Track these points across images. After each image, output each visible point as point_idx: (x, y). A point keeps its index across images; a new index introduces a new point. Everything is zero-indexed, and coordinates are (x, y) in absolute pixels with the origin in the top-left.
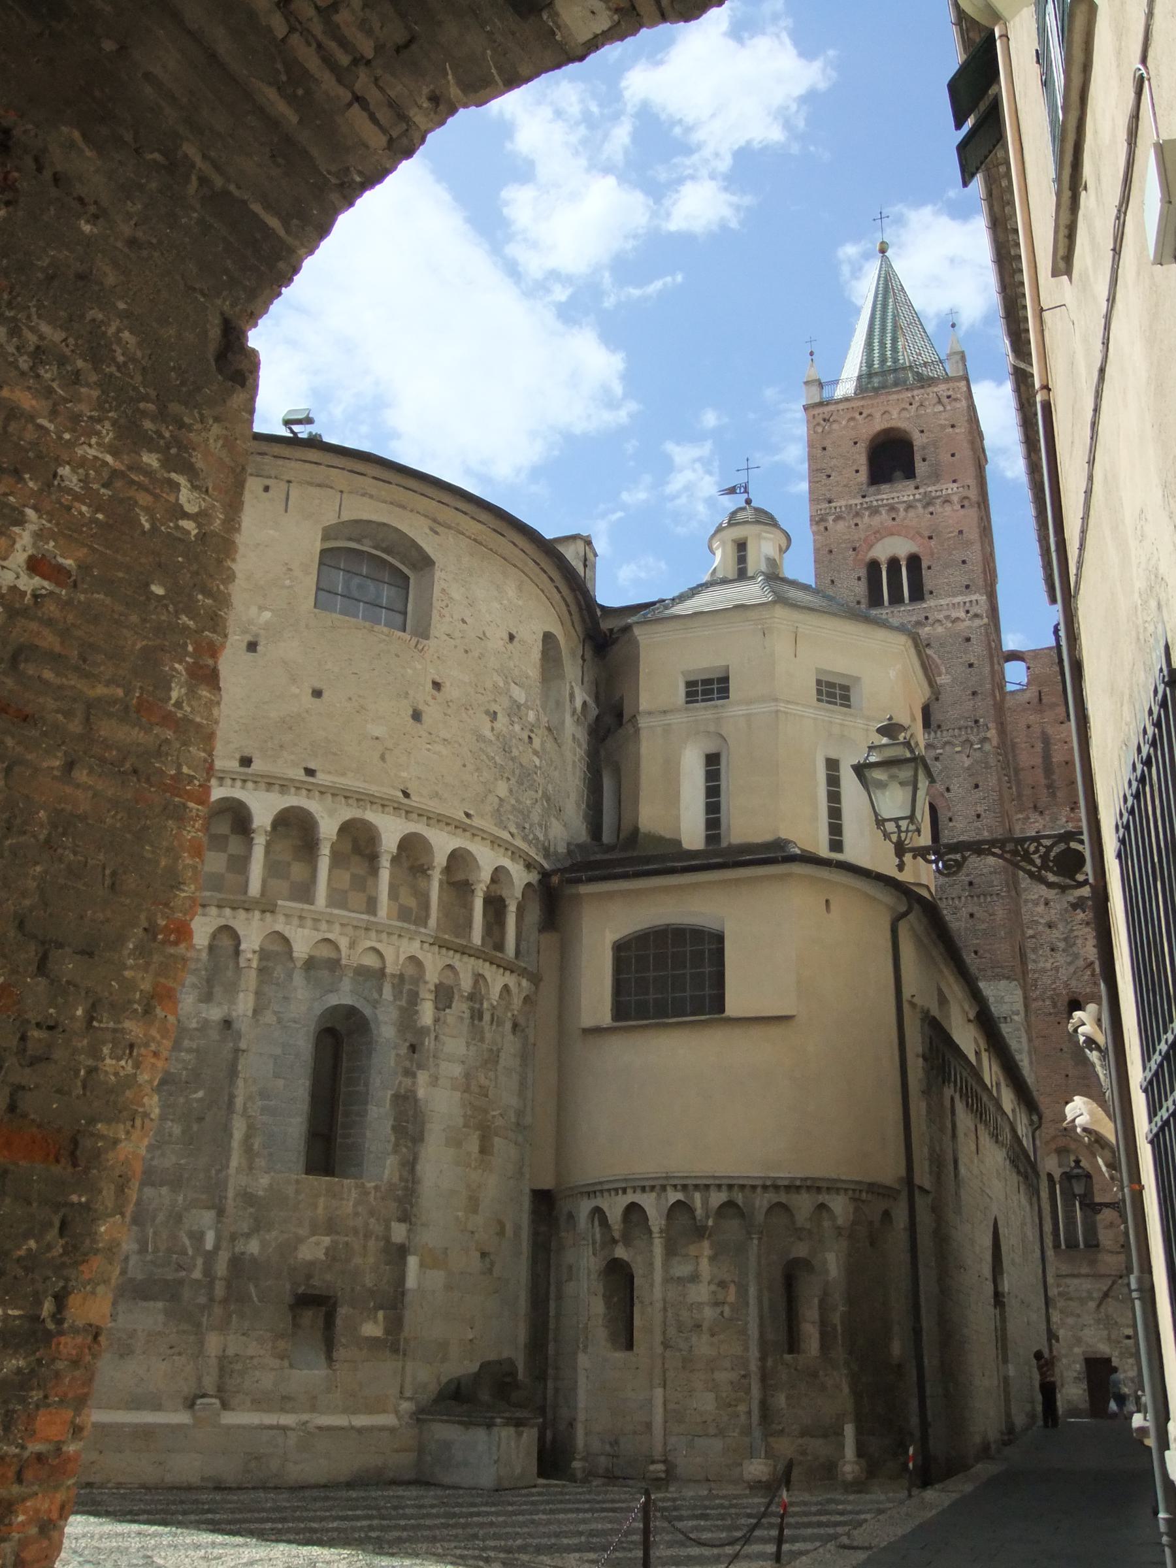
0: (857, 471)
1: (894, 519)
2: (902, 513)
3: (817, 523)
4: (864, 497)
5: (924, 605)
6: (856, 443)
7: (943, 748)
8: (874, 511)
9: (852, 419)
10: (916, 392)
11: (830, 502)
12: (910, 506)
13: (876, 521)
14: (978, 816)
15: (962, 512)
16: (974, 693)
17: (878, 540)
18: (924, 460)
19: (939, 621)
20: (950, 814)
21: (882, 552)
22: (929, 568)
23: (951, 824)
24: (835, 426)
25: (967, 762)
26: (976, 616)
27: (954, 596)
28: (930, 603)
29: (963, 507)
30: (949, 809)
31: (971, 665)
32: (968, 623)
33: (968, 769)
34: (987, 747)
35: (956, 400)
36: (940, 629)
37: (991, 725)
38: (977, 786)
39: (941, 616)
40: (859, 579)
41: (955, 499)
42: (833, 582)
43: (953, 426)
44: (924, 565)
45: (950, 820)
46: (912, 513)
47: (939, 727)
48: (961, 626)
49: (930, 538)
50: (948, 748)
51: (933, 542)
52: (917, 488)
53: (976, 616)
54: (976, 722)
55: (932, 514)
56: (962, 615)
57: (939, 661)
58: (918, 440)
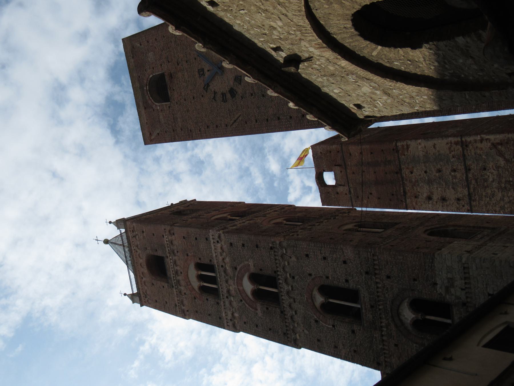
0: (163, 287)
1: (181, 273)
2: (178, 268)
3: (185, 315)
4: (173, 287)
5: (217, 266)
6: (153, 284)
7: (286, 273)
8: (178, 281)
9: (145, 282)
10: (133, 248)
11: (176, 305)
12: (175, 262)
13: (182, 283)
14: (325, 258)
15: (176, 235)
16: (257, 246)
17: (191, 284)
18: (156, 250)
19: (223, 259)
20: (324, 277)
21: (196, 284)
22: (200, 259)
23: (330, 278)
24: (148, 293)
25: (294, 259)
26: (219, 237)
27: (211, 248)
28: (215, 262)
29: (174, 234)
30: (322, 277)
31: (243, 245)
32: (223, 243)
33: (298, 259)
34: (285, 244)
35: (134, 227)
36: (227, 260)
37: (273, 240)
38: (307, 255)
39: (221, 258)
40: (207, 299)
41: (170, 238)
42: (209, 315)
43: (143, 232)
44: (199, 261)
45: (327, 277)
46: (178, 262)
47: (275, 272)
48: (225, 247)
49: (187, 255)
50: (287, 270)
51: (189, 254)
52: (167, 257)
53: (219, 237)
54: (271, 248)
55: (178, 252)
56: (219, 245)
57: (242, 264)
58: (149, 252)
